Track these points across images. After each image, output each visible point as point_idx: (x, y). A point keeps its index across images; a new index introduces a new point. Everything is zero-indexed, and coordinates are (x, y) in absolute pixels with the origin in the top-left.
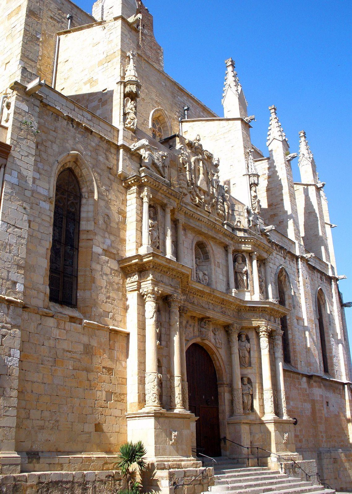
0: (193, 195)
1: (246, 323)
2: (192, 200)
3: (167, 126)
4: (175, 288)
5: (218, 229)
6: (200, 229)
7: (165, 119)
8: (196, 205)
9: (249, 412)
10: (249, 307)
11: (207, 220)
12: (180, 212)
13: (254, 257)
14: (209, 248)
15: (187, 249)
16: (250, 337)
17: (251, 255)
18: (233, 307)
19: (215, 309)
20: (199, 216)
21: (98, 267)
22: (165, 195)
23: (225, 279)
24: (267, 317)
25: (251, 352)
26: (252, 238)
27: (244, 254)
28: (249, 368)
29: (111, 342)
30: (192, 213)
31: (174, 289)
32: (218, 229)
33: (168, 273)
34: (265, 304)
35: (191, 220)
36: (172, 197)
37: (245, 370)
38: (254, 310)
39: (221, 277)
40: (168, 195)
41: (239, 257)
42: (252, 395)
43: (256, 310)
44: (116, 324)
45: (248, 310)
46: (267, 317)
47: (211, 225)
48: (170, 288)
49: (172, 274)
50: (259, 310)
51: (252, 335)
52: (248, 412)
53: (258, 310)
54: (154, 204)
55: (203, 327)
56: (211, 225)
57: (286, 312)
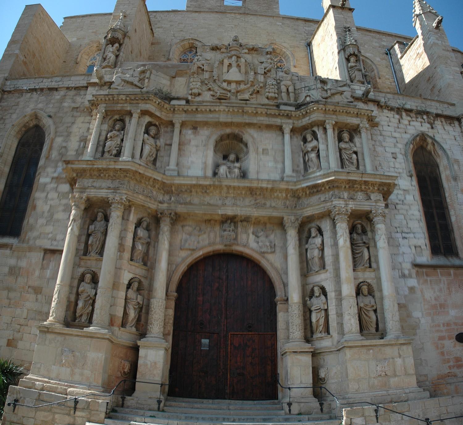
0: (213, 91)
1: (308, 212)
2: (213, 96)
3: (287, 55)
4: (114, 189)
5: (250, 111)
6: (217, 120)
7: (283, 50)
8: (220, 99)
9: (322, 336)
10: (308, 187)
11: (225, 107)
12: (176, 112)
13: (328, 127)
14: (246, 138)
15: (197, 146)
16: (323, 229)
17: (325, 126)
18: (280, 195)
19: (238, 203)
20: (209, 107)
21: (43, 195)
22: (130, 103)
23: (280, 166)
24: (346, 195)
25: (326, 249)
26: (314, 106)
27: (315, 129)
28: (322, 271)
29: (45, 262)
30: (195, 107)
31: (112, 191)
32: (250, 111)
33: (102, 175)
34: (329, 177)
35: (199, 115)
36: (140, 101)
37: (318, 276)
38: (317, 191)
39: (271, 164)
40: (133, 102)
41: (304, 133)
42: (326, 310)
43: (321, 190)
44: (55, 243)
45: (310, 192)
46: (346, 195)
47: (236, 110)
48: (107, 191)
49: (109, 176)
50: (325, 188)
51: (326, 226)
52: (319, 335)
53: (323, 189)
54: (120, 117)
55: (225, 230)
56: (236, 110)
57: (384, 181)
